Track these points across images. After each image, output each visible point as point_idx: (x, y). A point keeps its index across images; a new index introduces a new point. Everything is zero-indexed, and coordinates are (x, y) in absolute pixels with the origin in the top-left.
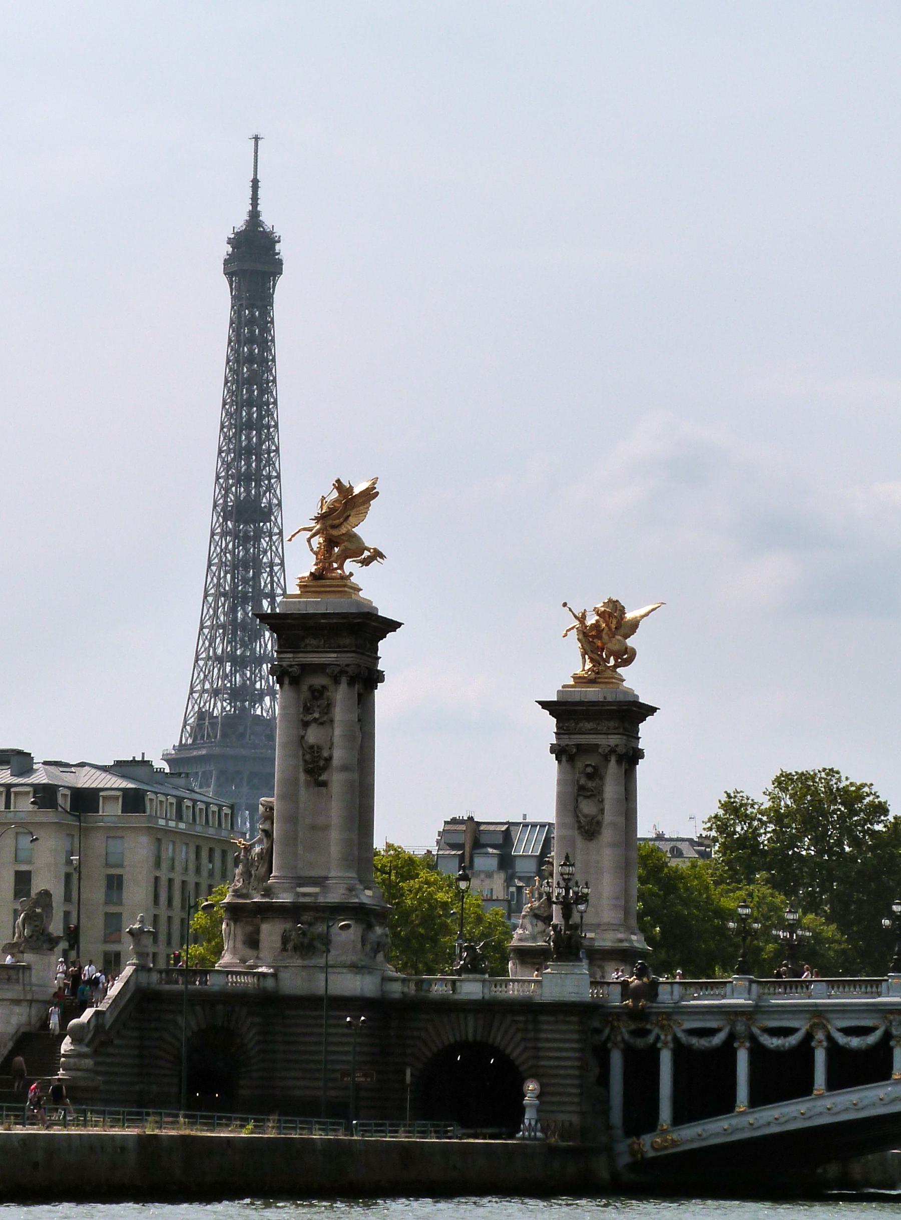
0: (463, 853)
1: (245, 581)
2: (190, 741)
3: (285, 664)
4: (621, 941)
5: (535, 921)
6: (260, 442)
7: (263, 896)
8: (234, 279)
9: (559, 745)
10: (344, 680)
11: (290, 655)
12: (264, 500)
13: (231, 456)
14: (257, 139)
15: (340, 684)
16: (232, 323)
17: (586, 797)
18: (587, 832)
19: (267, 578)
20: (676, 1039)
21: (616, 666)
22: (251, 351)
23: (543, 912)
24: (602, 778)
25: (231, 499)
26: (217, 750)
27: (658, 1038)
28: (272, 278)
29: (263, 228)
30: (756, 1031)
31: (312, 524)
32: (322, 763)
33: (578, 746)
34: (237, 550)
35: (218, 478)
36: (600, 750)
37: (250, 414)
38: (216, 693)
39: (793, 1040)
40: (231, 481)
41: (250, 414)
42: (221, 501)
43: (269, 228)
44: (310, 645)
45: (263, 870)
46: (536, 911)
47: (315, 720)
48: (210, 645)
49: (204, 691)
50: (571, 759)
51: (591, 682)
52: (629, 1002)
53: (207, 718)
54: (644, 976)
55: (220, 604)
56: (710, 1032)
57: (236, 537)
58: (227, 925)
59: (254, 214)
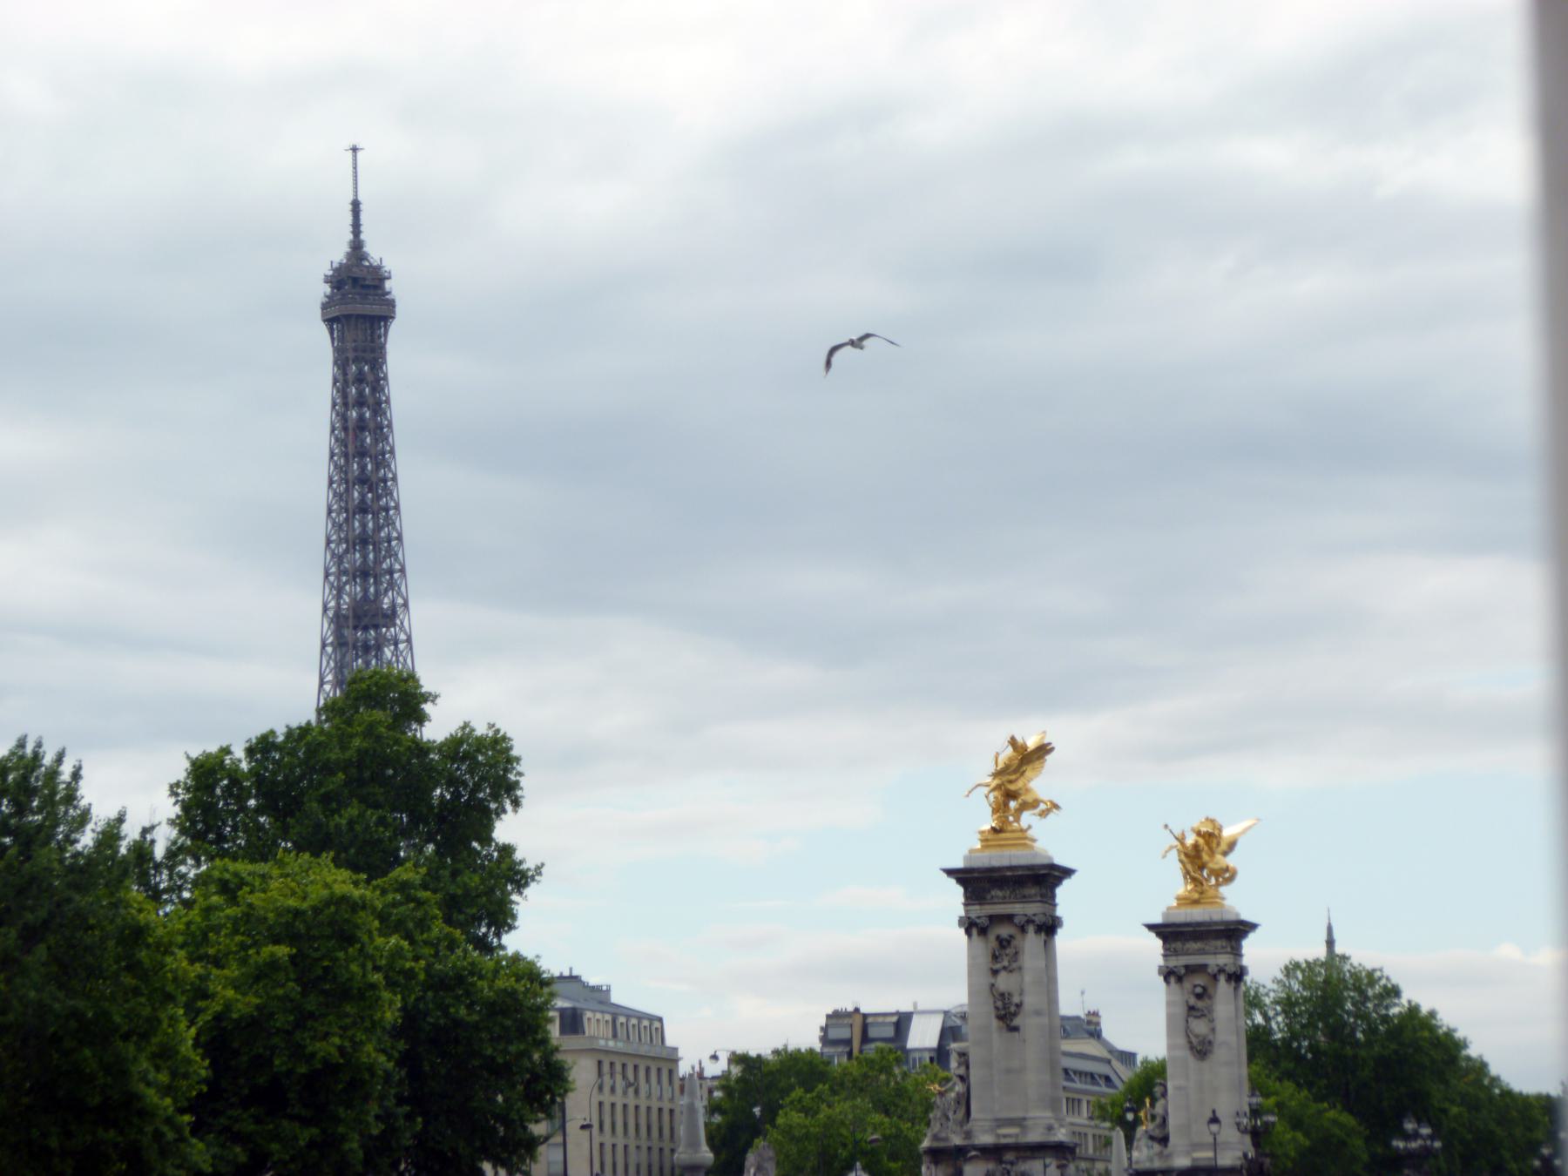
3: (973, 915)
5: (1150, 1143)
8: (335, 326)
10: (1031, 929)
11: (977, 907)
12: (386, 600)
14: (355, 150)
15: (1027, 933)
16: (335, 381)
17: (1196, 1017)
18: (1199, 1052)
21: (1218, 885)
22: (361, 418)
23: (1157, 1133)
24: (1210, 997)
28: (382, 324)
29: (369, 261)
31: (989, 780)
32: (1013, 1009)
33: (1187, 967)
34: (355, 664)
35: (327, 575)
40: (344, 579)
42: (332, 604)
44: (997, 897)
45: (961, 1113)
46: (1152, 1133)
47: (1005, 968)
50: (1180, 979)
51: (1196, 902)
58: (928, 1168)
59: (357, 246)
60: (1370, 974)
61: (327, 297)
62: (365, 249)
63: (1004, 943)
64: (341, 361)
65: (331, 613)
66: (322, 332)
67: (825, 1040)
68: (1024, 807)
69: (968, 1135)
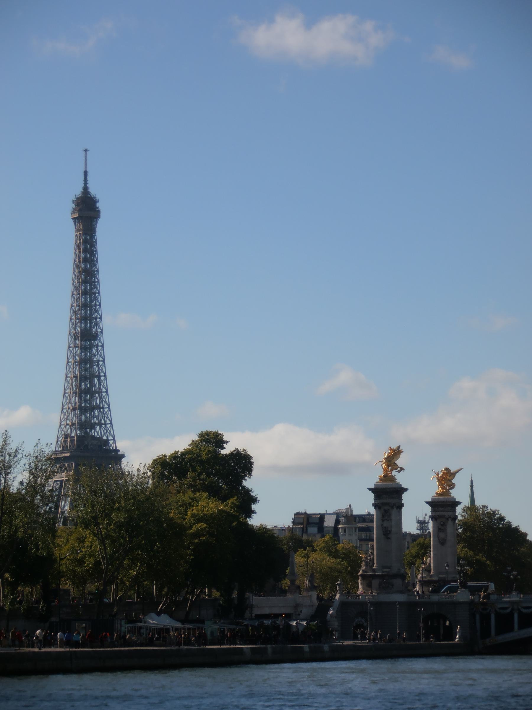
0: (303, 527)
2: (60, 449)
4: (454, 577)
7: (373, 572)
8: (76, 221)
9: (432, 516)
12: (94, 330)
13: (77, 308)
14: (86, 151)
15: (393, 508)
19: (96, 368)
21: (449, 489)
25: (78, 330)
27: (490, 610)
28: (95, 220)
29: (90, 195)
30: (520, 607)
33: (438, 515)
34: (81, 354)
35: (71, 319)
36: (445, 517)
40: (78, 321)
43: (93, 195)
47: (386, 519)
48: (69, 402)
50: (436, 520)
53: (69, 438)
54: (485, 593)
55: (74, 381)
56: (506, 608)
59: (86, 189)
60: (494, 512)
61: (74, 209)
62: (89, 190)
63: (386, 511)
65: (72, 335)
66: (72, 223)
67: (294, 523)
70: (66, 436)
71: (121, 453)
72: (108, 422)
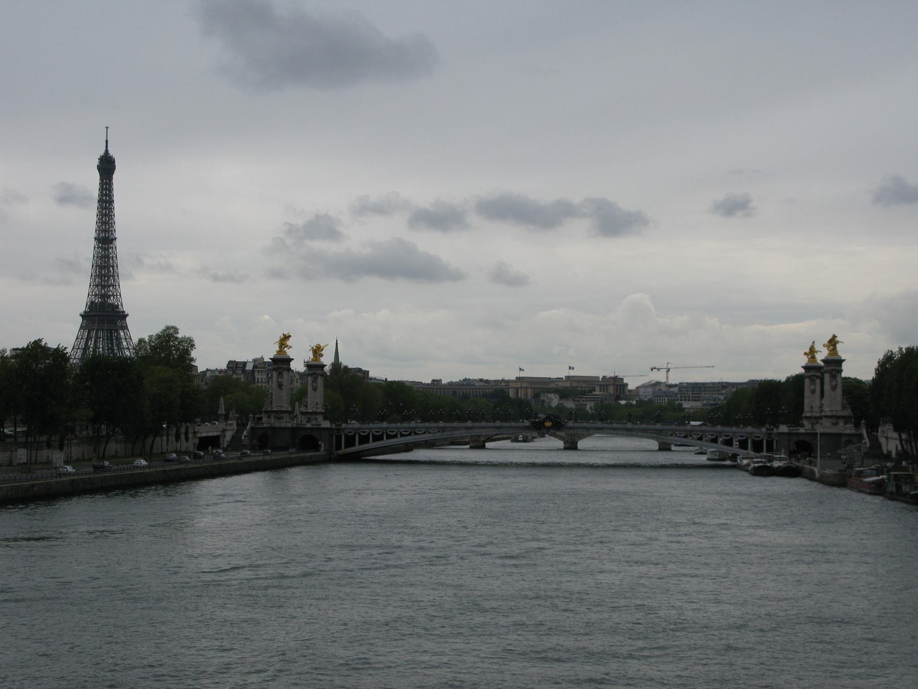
1: (105, 262)
6: (109, 220)
10: (285, 370)
14: (107, 128)
20: (345, 434)
22: (106, 193)
26: (98, 313)
35: (96, 231)
37: (106, 212)
38: (96, 295)
39: (366, 434)
41: (106, 212)
49: (92, 295)
50: (311, 376)
51: (315, 361)
52: (337, 427)
57: (102, 249)
59: (107, 151)
63: (280, 373)
64: (102, 179)
68: (285, 347)
69: (272, 408)
70: (92, 303)
71: (126, 313)
72: (118, 294)
